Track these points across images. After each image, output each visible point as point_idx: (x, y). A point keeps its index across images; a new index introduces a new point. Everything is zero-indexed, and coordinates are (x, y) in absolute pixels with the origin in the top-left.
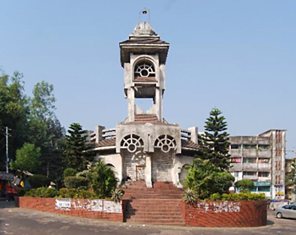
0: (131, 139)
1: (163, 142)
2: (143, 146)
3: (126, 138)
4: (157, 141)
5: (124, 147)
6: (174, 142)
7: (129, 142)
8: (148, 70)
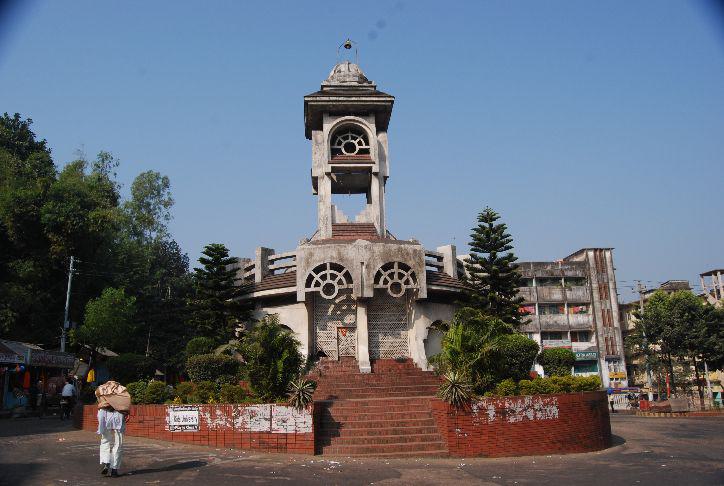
0: (329, 272)
1: (391, 276)
2: (351, 286)
3: (317, 270)
4: (378, 275)
5: (312, 289)
6: (413, 275)
7: (324, 277)
8: (356, 142)
